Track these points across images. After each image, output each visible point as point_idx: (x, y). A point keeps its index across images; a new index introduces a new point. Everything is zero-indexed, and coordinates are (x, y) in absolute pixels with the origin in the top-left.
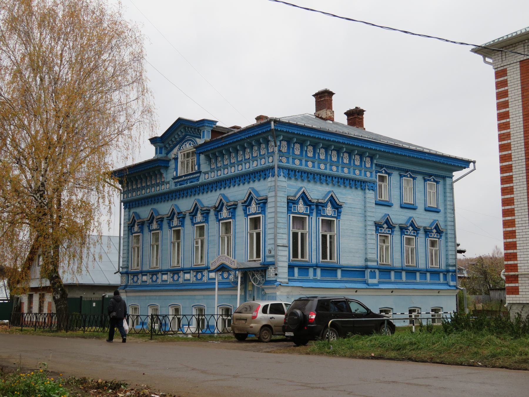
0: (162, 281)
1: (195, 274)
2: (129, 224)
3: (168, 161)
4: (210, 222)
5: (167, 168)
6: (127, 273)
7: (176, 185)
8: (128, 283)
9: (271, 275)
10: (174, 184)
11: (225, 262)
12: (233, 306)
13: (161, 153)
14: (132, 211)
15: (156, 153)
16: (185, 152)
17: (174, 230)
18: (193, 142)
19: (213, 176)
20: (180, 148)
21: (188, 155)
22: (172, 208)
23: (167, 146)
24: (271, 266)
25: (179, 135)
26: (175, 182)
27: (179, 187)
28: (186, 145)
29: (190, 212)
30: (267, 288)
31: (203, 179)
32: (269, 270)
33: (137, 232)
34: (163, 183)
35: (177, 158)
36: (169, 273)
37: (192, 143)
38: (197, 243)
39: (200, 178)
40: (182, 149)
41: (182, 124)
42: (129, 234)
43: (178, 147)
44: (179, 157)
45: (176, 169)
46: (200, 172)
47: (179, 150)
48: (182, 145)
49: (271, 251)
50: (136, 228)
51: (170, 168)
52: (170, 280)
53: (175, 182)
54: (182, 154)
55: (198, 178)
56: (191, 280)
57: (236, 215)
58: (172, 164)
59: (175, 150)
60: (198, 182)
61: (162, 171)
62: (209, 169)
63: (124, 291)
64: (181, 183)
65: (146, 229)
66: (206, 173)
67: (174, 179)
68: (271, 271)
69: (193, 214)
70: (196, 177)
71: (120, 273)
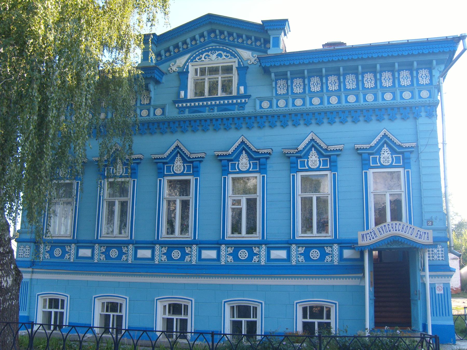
5: (157, 82)
7: (181, 110)
9: (436, 257)
10: (177, 110)
16: (207, 66)
18: (228, 52)
20: (195, 58)
21: (214, 71)
23: (163, 52)
26: (178, 108)
27: (187, 114)
35: (187, 72)
37: (224, 54)
39: (246, 106)
41: (211, 23)
43: (187, 56)
44: (189, 70)
48: (198, 55)
53: (178, 108)
54: (198, 67)
55: (242, 106)
59: (181, 61)
62: (274, 95)
66: (262, 100)
67: (175, 102)
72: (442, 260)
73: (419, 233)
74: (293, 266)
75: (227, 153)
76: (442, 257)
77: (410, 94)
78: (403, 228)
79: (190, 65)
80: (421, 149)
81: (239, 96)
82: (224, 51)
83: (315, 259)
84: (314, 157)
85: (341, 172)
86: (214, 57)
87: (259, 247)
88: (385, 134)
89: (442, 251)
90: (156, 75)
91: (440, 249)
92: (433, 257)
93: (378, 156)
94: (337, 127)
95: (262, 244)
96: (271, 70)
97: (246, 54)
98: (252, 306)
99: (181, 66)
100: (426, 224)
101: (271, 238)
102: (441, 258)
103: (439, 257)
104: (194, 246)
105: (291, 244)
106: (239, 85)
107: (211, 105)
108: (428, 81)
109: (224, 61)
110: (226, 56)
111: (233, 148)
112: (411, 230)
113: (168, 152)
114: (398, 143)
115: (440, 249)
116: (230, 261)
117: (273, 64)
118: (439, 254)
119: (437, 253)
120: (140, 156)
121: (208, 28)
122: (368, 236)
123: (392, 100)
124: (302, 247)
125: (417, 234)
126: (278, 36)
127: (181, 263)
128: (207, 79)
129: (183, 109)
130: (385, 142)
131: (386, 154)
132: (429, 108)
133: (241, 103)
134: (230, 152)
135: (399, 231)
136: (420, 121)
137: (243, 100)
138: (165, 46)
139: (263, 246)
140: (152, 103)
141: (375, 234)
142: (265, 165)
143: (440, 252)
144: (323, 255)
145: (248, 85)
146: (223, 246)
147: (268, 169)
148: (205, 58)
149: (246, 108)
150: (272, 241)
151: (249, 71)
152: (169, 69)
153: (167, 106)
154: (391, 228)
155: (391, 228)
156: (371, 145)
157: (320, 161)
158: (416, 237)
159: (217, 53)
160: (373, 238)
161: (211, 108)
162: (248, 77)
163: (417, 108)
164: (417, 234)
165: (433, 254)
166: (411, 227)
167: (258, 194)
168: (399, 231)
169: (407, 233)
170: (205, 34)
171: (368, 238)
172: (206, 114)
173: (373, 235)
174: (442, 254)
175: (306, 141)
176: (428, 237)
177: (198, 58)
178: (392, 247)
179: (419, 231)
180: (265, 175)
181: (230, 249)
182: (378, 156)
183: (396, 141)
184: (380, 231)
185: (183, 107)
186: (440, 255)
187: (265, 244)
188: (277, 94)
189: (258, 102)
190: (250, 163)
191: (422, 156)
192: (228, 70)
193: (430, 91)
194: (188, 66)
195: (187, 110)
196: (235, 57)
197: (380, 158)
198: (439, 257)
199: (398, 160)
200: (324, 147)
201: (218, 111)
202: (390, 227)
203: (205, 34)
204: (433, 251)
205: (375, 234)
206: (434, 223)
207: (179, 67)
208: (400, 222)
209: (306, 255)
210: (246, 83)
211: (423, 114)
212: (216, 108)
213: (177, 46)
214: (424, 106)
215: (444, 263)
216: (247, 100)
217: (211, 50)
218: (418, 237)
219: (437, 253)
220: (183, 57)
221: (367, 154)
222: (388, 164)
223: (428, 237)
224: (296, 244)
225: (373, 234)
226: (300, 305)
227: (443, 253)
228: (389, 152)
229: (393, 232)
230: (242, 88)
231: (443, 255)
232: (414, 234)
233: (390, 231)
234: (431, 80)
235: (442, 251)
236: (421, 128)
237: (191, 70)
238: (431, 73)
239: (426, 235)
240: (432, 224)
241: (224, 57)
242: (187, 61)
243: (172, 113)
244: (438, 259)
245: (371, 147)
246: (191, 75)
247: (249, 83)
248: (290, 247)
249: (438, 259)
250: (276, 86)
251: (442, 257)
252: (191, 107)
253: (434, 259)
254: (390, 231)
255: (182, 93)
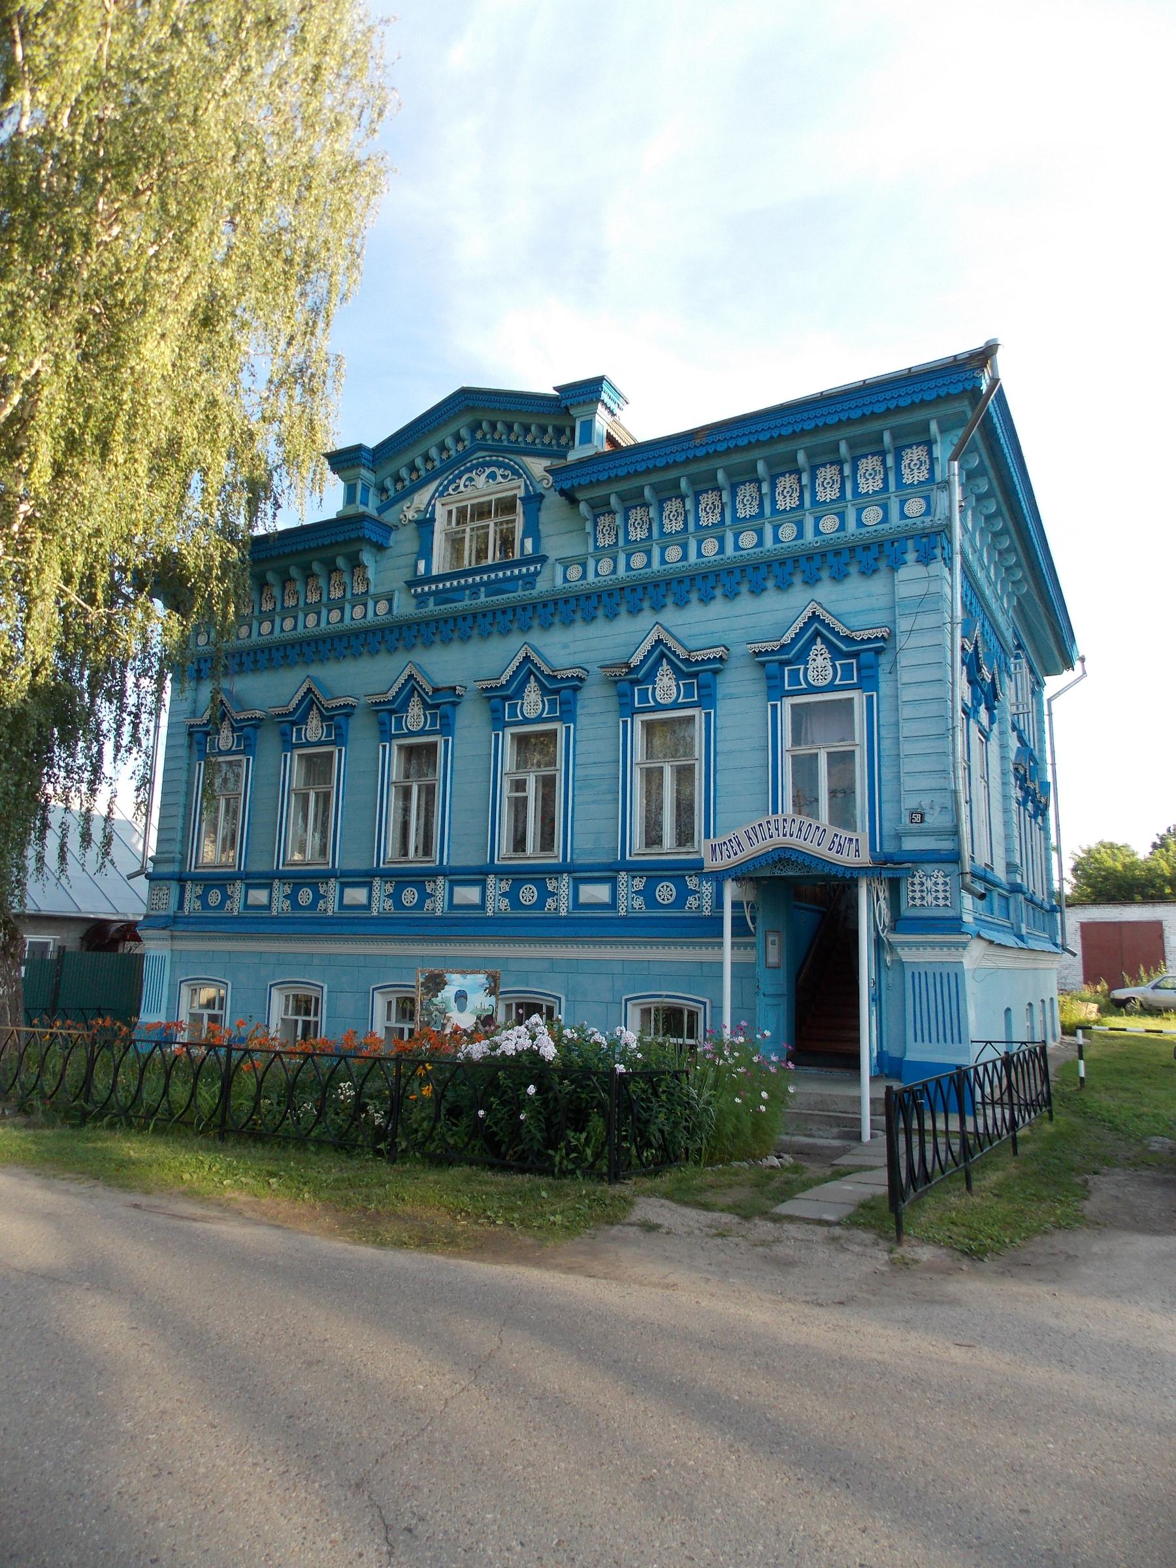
0: (247, 907)
1: (390, 888)
2: (191, 726)
3: (389, 529)
4: (582, 720)
5: (380, 548)
6: (181, 879)
7: (421, 599)
8: (181, 906)
9: (929, 898)
11: (796, 842)
12: (711, 1002)
13: (365, 503)
14: (206, 690)
15: (350, 498)
16: (469, 503)
17: (400, 747)
18: (506, 467)
19: (602, 572)
20: (446, 488)
21: (482, 511)
22: (407, 672)
23: (388, 483)
24: (928, 868)
25: (442, 448)
26: (416, 596)
27: (431, 607)
28: (471, 479)
29: (493, 684)
30: (909, 945)
31: (551, 580)
32: (917, 880)
33: (229, 752)
34: (361, 600)
35: (432, 520)
36: (377, 882)
37: (499, 472)
38: (520, 785)
39: (538, 579)
40: (451, 491)
41: (470, 409)
42: (190, 758)
43: (433, 486)
44: (437, 516)
45: (425, 552)
46: (543, 559)
47: (441, 495)
49: (922, 815)
50: (226, 738)
51: (388, 552)
52: (281, 906)
53: (416, 596)
54: (453, 507)
55: (530, 581)
56: (274, 907)
57: (719, 696)
58: (403, 542)
59: (422, 498)
60: (534, 592)
61: (366, 557)
62: (591, 549)
63: (167, 933)
64: (442, 597)
65: (268, 742)
66: (566, 563)
67: (410, 584)
68: (929, 884)
69: (509, 692)
70: (521, 576)
71: (148, 876)
72: (946, 905)
73: (837, 840)
74: (705, 917)
75: (498, 683)
76: (946, 898)
77: (881, 512)
78: (800, 830)
79: (438, 505)
80: (901, 641)
81: (526, 561)
82: (500, 465)
83: (666, 902)
84: (666, 679)
85: (723, 706)
86: (481, 481)
87: (556, 879)
88: (814, 613)
89: (945, 884)
90: (367, 532)
91: (940, 881)
92: (922, 898)
93: (802, 667)
94: (718, 607)
95: (562, 873)
96: (580, 496)
97: (538, 466)
98: (544, 1004)
99: (423, 507)
100: (908, 821)
101: (582, 860)
102: (941, 902)
103: (937, 898)
104: (441, 878)
105: (618, 871)
106: (525, 536)
107: (475, 585)
108: (923, 475)
109: (501, 487)
110: (504, 476)
111: (509, 673)
112: (818, 833)
113: (395, 689)
114: (843, 631)
115: (940, 881)
116: (503, 908)
117: (576, 482)
118: (937, 891)
119: (934, 888)
120: (350, 701)
121: (467, 419)
122: (724, 848)
123: (837, 531)
124: (641, 877)
125: (833, 842)
126: (589, 418)
127: (417, 914)
128: (468, 530)
129: (423, 598)
130: (818, 633)
131: (819, 659)
132: (924, 540)
133: (528, 575)
134: (503, 680)
135: (791, 835)
136: (903, 573)
137: (532, 569)
138: (391, 468)
139: (565, 875)
140: (372, 590)
141: (739, 844)
142: (569, 703)
143: (940, 888)
144: (684, 893)
145: (543, 534)
146: (492, 876)
147: (579, 711)
148: (466, 486)
149: (538, 585)
150: (581, 865)
151: (546, 502)
152: (402, 516)
153: (396, 595)
154: (773, 830)
155: (773, 830)
156: (782, 641)
157: (678, 686)
158: (830, 849)
159: (488, 471)
160: (736, 854)
161: (474, 589)
162: (544, 516)
163: (896, 544)
164: (833, 842)
165: (922, 891)
166: (818, 828)
167: (558, 767)
168: (791, 835)
169: (809, 839)
170: (464, 433)
171: (725, 853)
172: (465, 603)
173: (736, 847)
174: (945, 891)
175: (646, 646)
176: (857, 851)
177: (453, 486)
178: (784, 874)
179: (836, 835)
180: (572, 726)
181: (504, 883)
182: (802, 667)
183: (839, 627)
184: (750, 838)
185: (424, 594)
186: (941, 895)
187: (569, 873)
188: (596, 547)
189: (559, 569)
190: (543, 701)
191: (903, 660)
192: (507, 506)
193: (927, 499)
194: (434, 506)
195: (432, 599)
196: (520, 476)
197: (806, 670)
198: (937, 898)
199: (847, 671)
200: (683, 655)
201: (486, 596)
202: (772, 826)
203: (464, 433)
204: (922, 884)
205: (739, 844)
206: (927, 818)
207: (418, 511)
208: (811, 821)
209: (648, 894)
210: (538, 531)
211: (911, 556)
212: (483, 589)
213: (413, 468)
214: (912, 537)
215: (950, 913)
216: (539, 566)
217: (476, 467)
218: (835, 850)
219: (934, 888)
220: (425, 489)
221: (777, 664)
222: (825, 682)
223: (857, 851)
224: (627, 871)
225: (734, 844)
226: (634, 1005)
227: (948, 888)
228: (828, 656)
229: (779, 840)
230: (529, 543)
231: (948, 894)
232: (826, 843)
233: (771, 837)
234: (931, 471)
235: (945, 884)
236: (903, 591)
237: (440, 513)
238: (930, 452)
239: (854, 844)
240: (922, 821)
241: (500, 479)
242: (432, 497)
243: (404, 606)
244: (935, 903)
245: (783, 646)
246: (439, 526)
247: (544, 529)
248: (616, 878)
249: (935, 903)
250: (595, 530)
251: (946, 898)
252: (437, 593)
253: (925, 903)
254: (771, 837)
255: (422, 565)
